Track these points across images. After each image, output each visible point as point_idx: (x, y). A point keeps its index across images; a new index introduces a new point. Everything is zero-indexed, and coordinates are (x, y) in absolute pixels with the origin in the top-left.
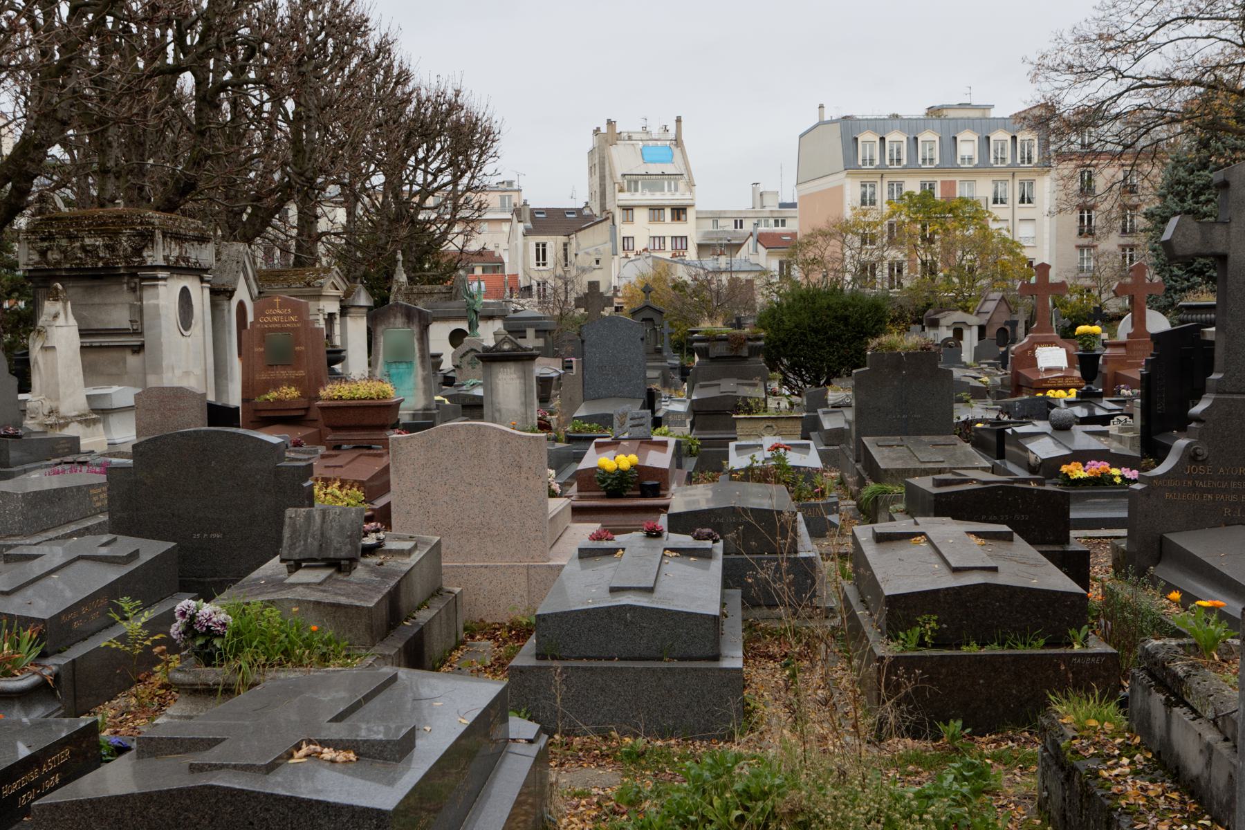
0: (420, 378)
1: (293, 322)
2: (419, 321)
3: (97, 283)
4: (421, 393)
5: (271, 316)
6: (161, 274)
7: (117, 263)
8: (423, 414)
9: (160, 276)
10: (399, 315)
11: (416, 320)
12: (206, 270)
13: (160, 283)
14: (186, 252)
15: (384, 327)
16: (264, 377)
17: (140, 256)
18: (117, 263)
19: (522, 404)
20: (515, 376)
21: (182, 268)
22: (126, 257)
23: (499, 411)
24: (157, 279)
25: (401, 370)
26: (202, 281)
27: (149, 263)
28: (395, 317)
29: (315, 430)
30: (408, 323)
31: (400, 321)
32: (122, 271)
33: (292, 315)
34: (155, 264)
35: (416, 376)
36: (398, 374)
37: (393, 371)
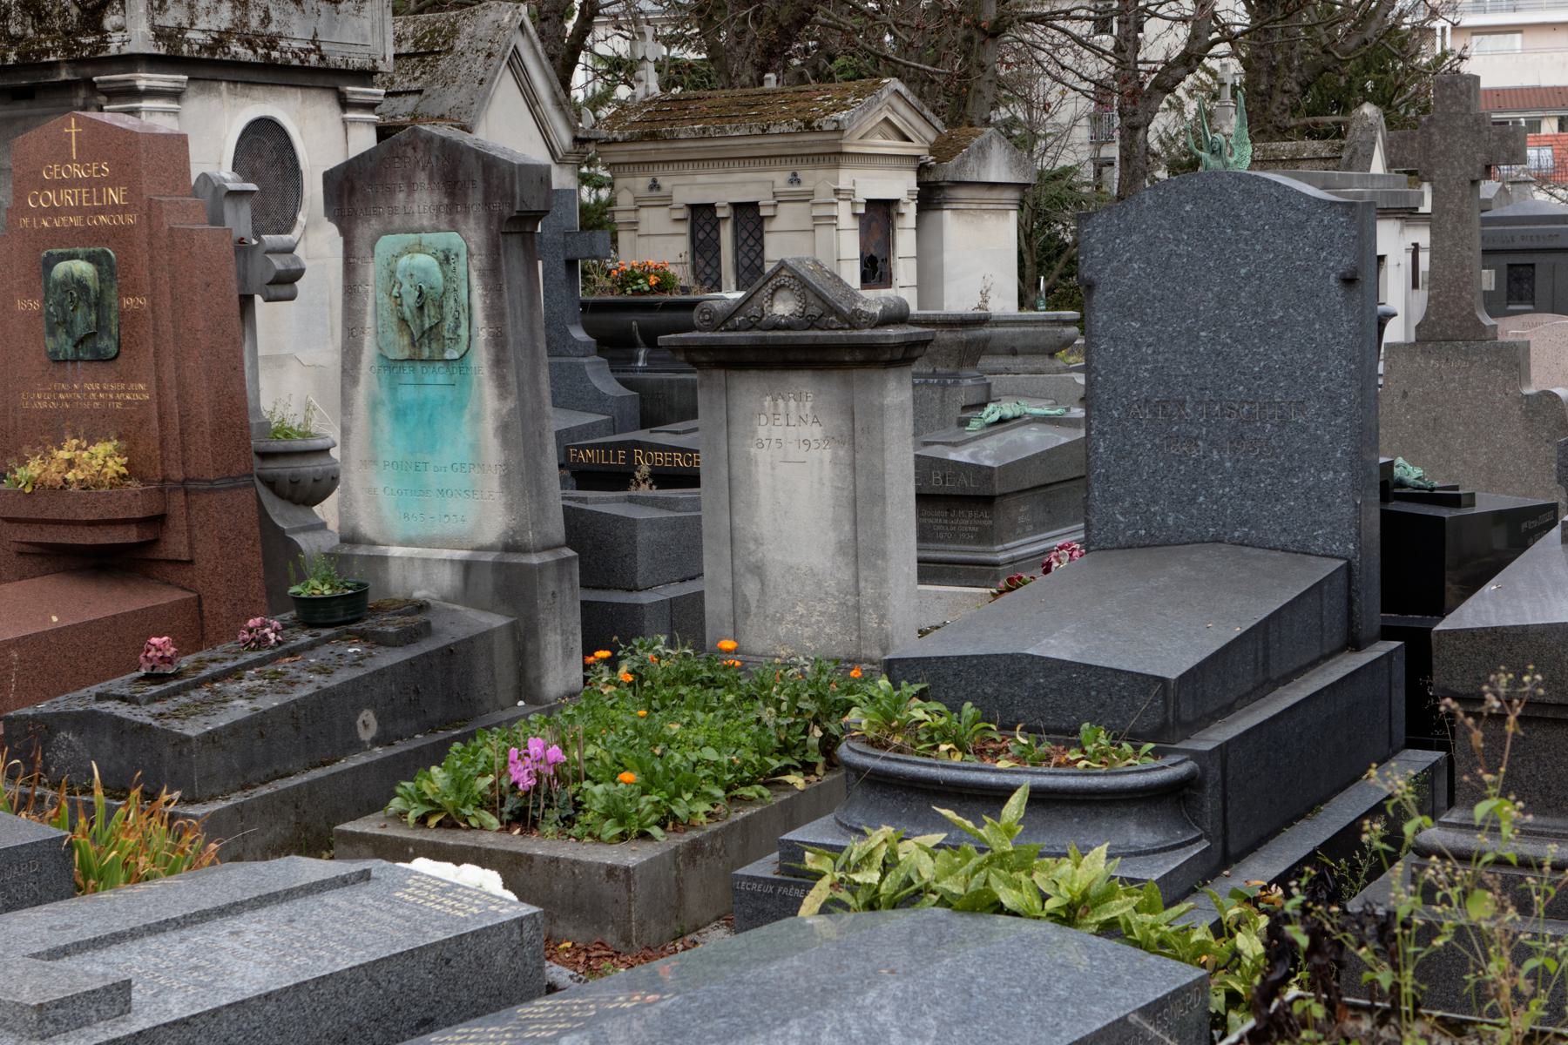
0: (489, 425)
1: (114, 209)
2: (487, 203)
3: (21, 109)
4: (493, 482)
5: (59, 185)
6: (144, 80)
7: (46, 52)
8: (498, 566)
9: (142, 84)
10: (422, 177)
11: (475, 197)
12: (365, 76)
13: (146, 104)
14: (266, 19)
15: (375, 224)
16: (41, 401)
17: (99, 30)
18: (46, 52)
19: (841, 548)
20: (815, 432)
21: (238, 65)
22: (68, 33)
23: (758, 570)
24: (133, 93)
25: (431, 393)
26: (345, 104)
27: (113, 50)
28: (411, 187)
29: (179, 595)
30: (451, 209)
31: (423, 201)
32: (64, 75)
33: (112, 182)
34: (126, 50)
35: (477, 418)
36: (422, 405)
37: (407, 393)
